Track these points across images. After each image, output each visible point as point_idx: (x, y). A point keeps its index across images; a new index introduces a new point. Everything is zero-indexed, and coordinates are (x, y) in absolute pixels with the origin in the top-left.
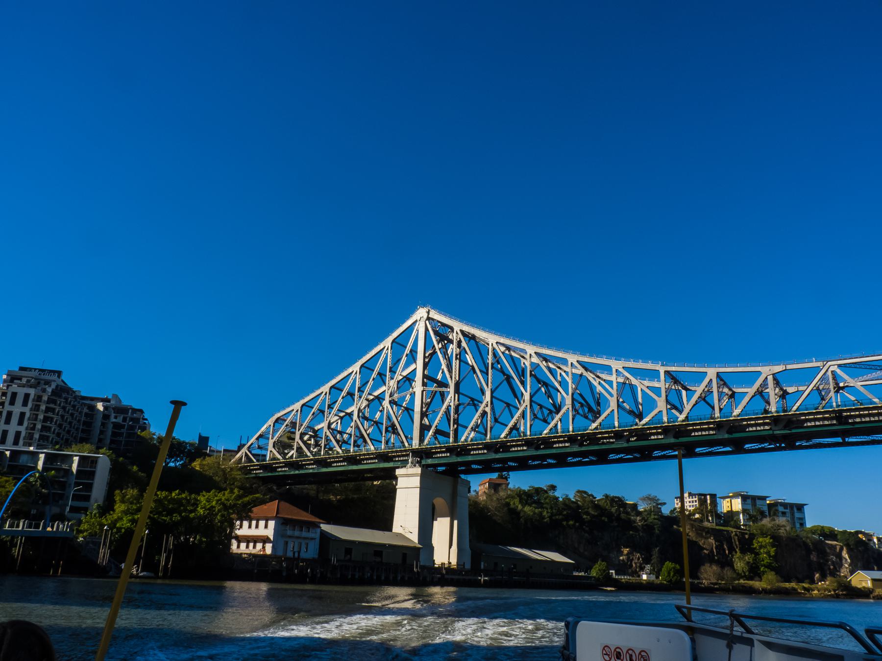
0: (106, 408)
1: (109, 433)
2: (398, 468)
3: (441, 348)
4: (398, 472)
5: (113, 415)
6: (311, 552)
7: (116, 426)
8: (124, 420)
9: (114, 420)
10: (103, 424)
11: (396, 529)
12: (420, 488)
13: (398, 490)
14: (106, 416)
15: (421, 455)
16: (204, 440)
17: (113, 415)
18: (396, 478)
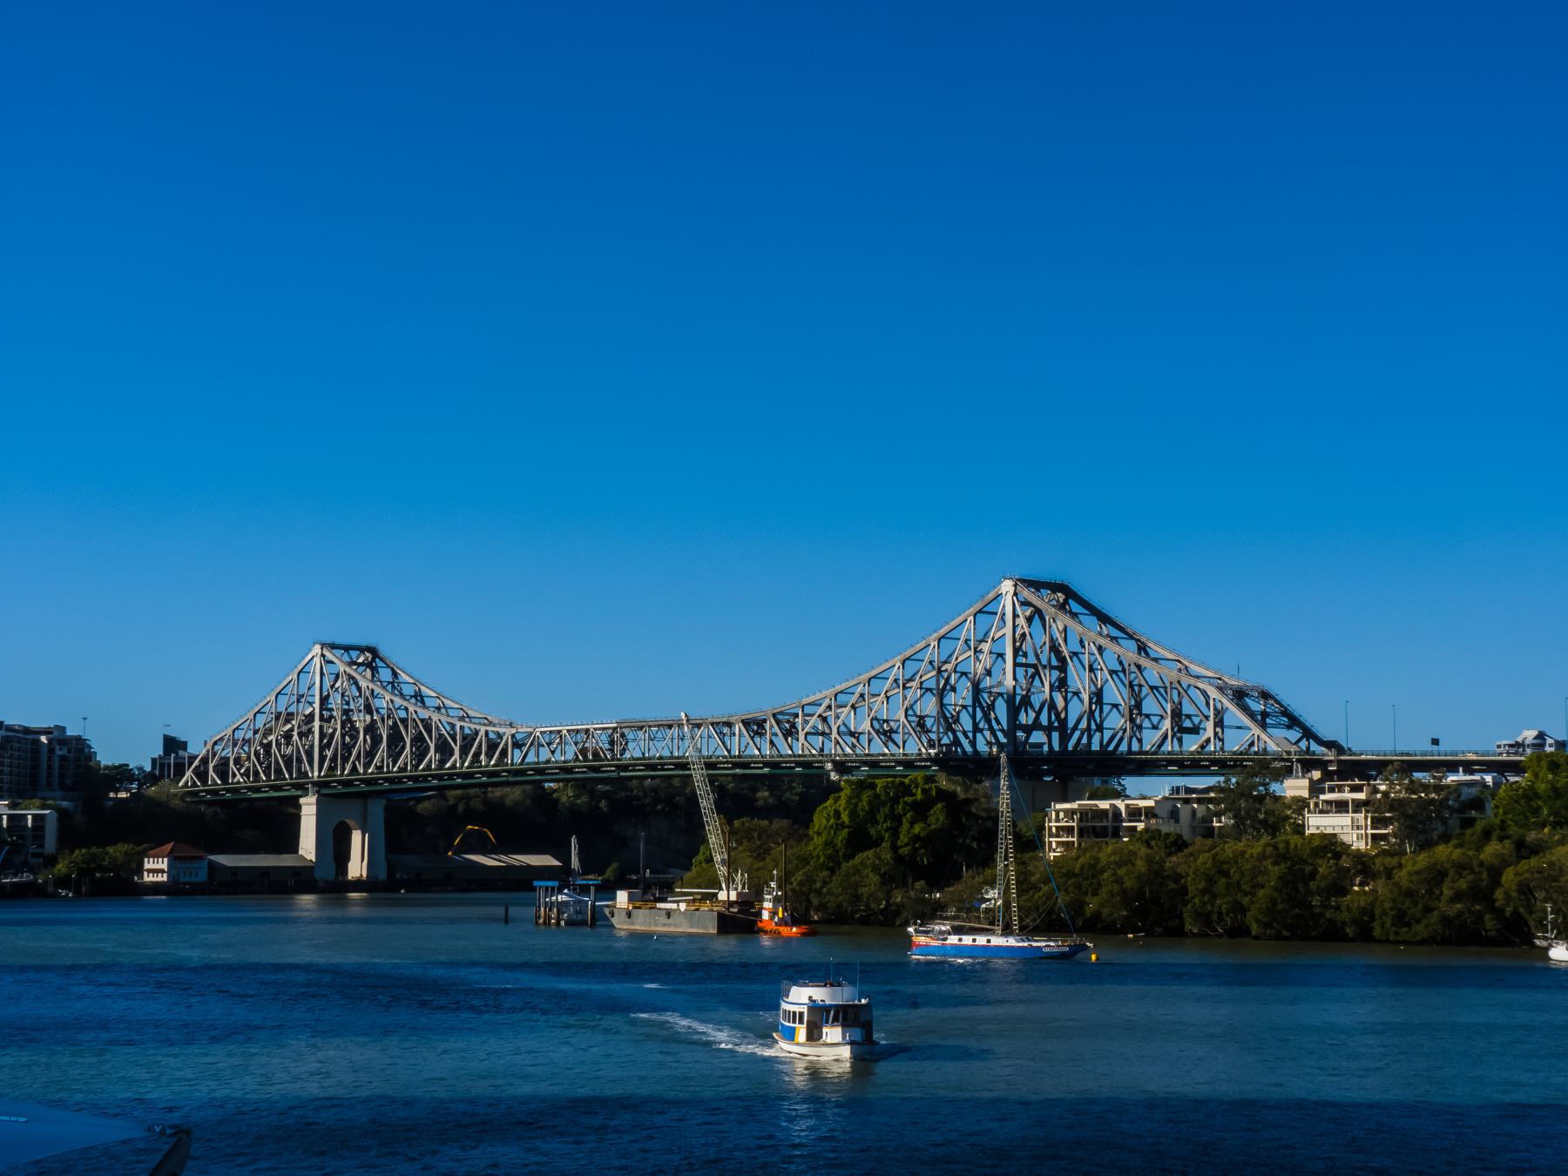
0: (50, 741)
1: (56, 765)
2: (301, 796)
3: (373, 660)
4: (302, 801)
5: (57, 747)
6: (202, 876)
7: (63, 758)
8: (69, 751)
9: (59, 753)
10: (50, 759)
11: (301, 852)
12: (317, 815)
13: (303, 819)
14: (51, 750)
15: (320, 785)
16: (172, 744)
17: (57, 747)
18: (299, 807)
